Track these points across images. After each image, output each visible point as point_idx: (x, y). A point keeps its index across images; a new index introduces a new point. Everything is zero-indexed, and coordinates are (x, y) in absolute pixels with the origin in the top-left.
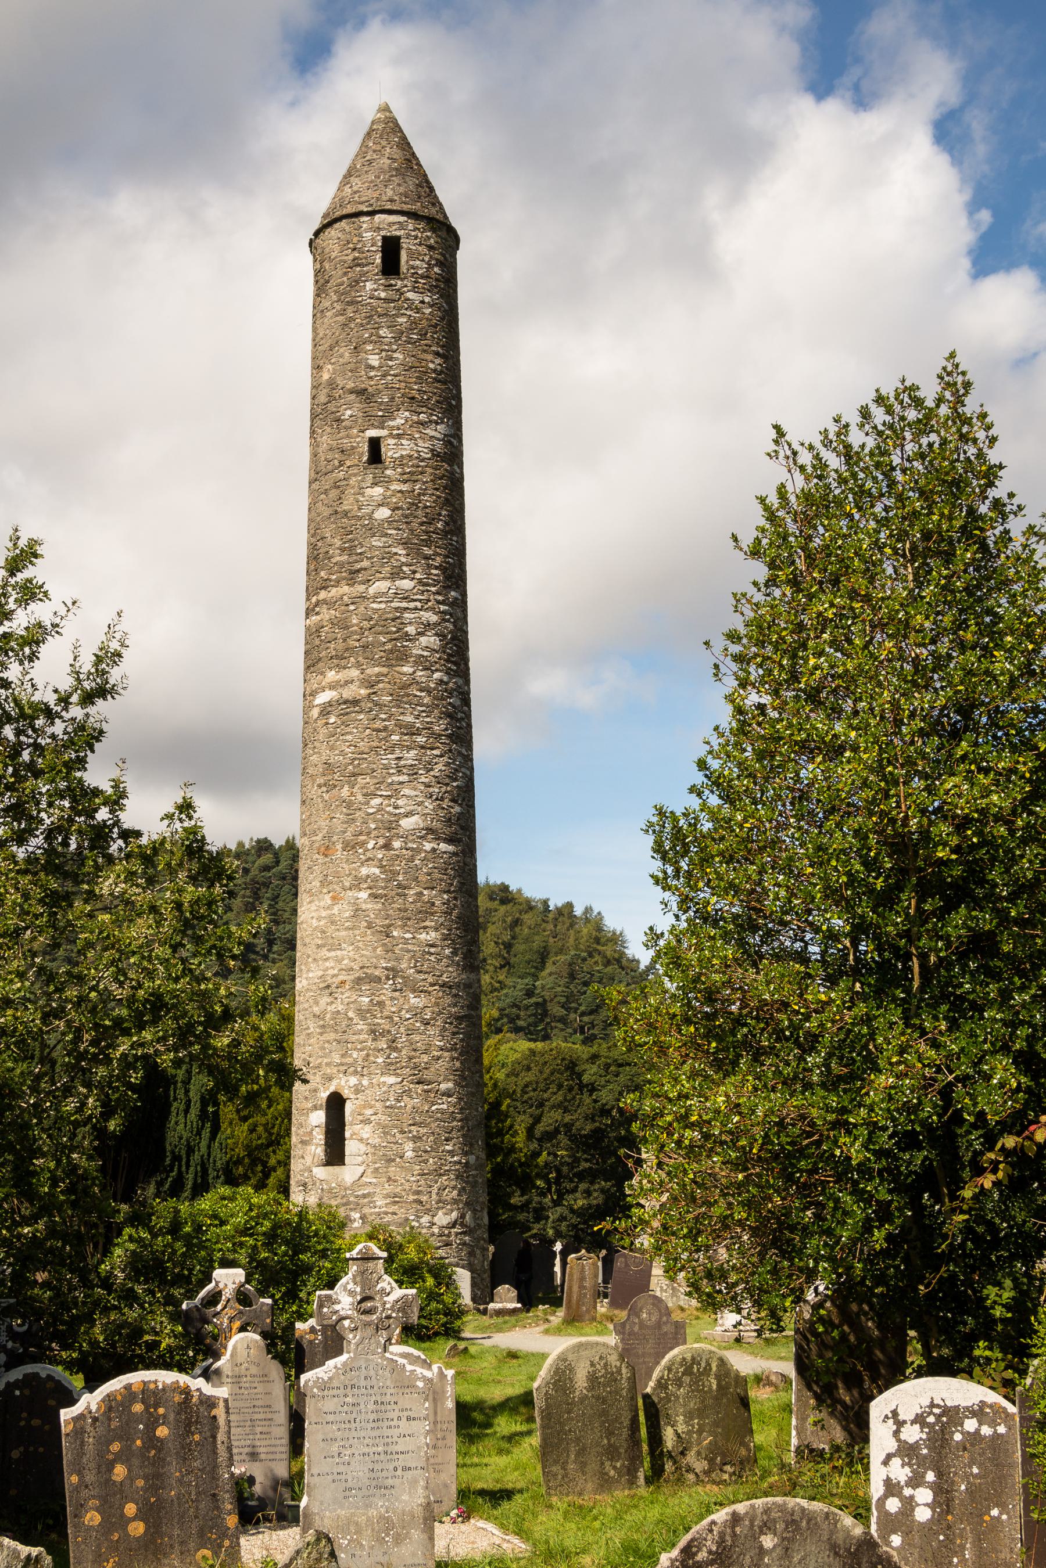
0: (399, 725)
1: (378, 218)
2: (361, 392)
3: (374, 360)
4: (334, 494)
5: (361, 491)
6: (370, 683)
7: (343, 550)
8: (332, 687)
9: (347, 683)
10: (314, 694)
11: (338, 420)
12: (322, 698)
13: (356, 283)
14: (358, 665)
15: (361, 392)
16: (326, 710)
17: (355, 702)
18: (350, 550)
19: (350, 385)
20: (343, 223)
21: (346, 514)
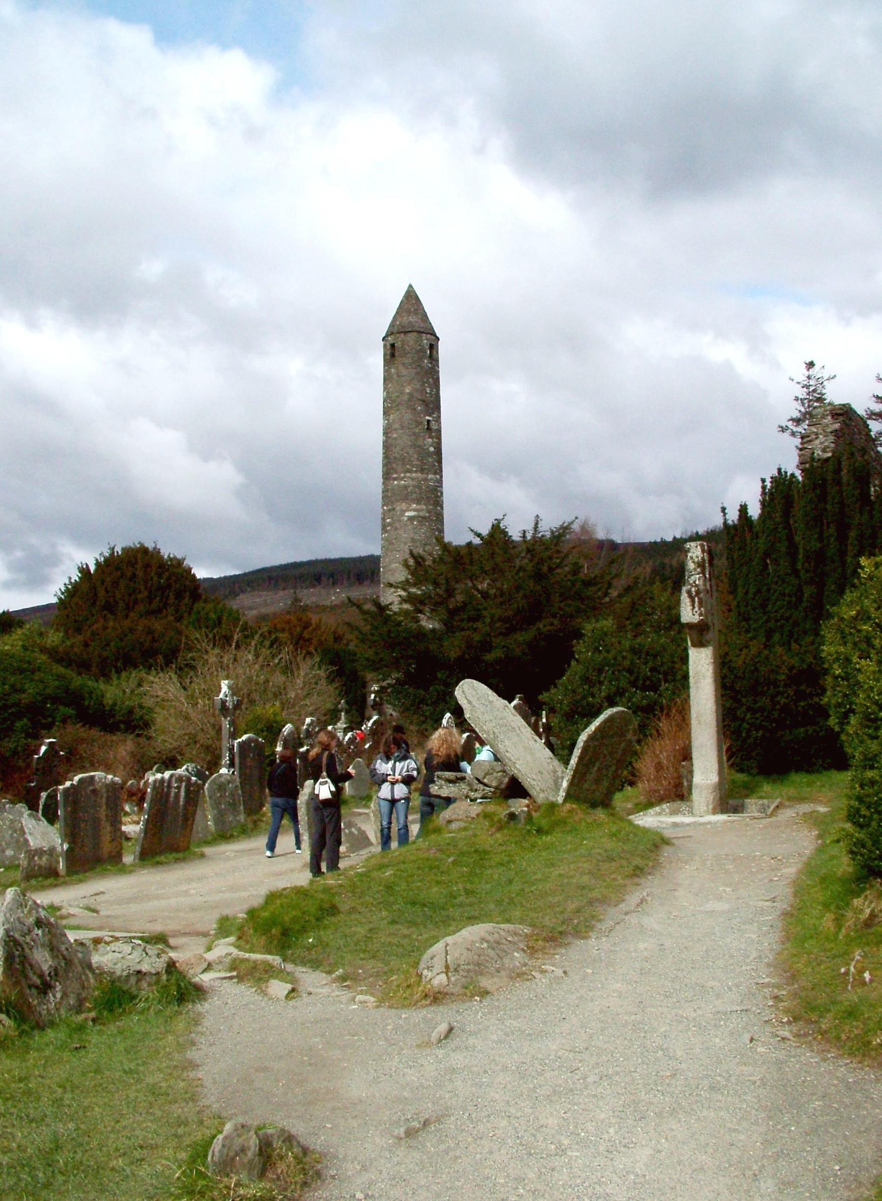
0: (438, 529)
1: (429, 336)
2: (424, 401)
3: (428, 390)
4: (413, 437)
5: (424, 439)
6: (429, 512)
7: (418, 459)
8: (414, 510)
9: (422, 510)
10: (405, 511)
11: (415, 409)
12: (407, 514)
13: (421, 359)
14: (425, 504)
15: (424, 401)
16: (411, 519)
17: (424, 518)
18: (422, 461)
19: (420, 397)
20: (415, 334)
21: (419, 446)
